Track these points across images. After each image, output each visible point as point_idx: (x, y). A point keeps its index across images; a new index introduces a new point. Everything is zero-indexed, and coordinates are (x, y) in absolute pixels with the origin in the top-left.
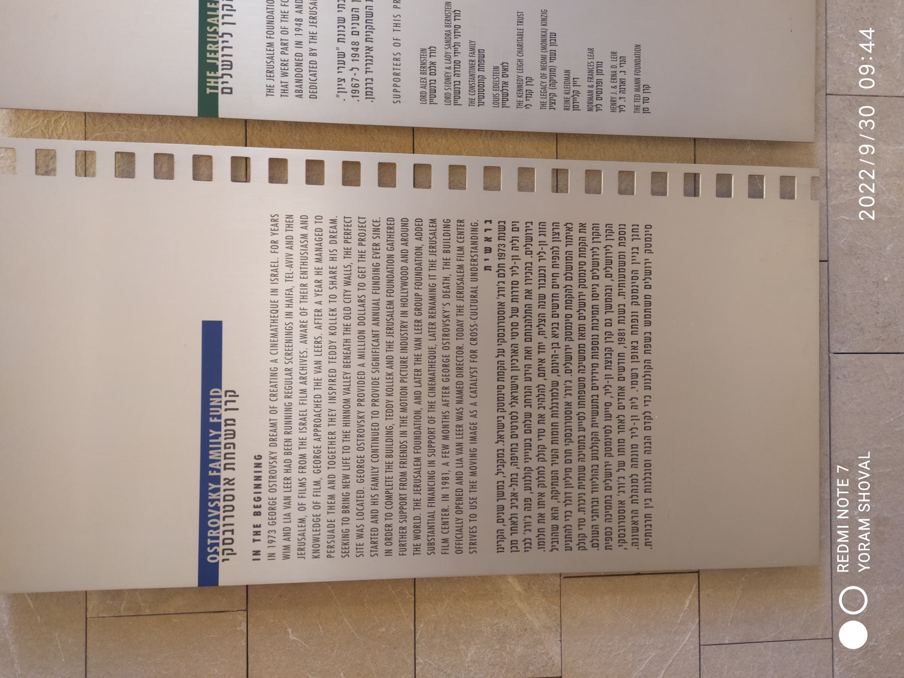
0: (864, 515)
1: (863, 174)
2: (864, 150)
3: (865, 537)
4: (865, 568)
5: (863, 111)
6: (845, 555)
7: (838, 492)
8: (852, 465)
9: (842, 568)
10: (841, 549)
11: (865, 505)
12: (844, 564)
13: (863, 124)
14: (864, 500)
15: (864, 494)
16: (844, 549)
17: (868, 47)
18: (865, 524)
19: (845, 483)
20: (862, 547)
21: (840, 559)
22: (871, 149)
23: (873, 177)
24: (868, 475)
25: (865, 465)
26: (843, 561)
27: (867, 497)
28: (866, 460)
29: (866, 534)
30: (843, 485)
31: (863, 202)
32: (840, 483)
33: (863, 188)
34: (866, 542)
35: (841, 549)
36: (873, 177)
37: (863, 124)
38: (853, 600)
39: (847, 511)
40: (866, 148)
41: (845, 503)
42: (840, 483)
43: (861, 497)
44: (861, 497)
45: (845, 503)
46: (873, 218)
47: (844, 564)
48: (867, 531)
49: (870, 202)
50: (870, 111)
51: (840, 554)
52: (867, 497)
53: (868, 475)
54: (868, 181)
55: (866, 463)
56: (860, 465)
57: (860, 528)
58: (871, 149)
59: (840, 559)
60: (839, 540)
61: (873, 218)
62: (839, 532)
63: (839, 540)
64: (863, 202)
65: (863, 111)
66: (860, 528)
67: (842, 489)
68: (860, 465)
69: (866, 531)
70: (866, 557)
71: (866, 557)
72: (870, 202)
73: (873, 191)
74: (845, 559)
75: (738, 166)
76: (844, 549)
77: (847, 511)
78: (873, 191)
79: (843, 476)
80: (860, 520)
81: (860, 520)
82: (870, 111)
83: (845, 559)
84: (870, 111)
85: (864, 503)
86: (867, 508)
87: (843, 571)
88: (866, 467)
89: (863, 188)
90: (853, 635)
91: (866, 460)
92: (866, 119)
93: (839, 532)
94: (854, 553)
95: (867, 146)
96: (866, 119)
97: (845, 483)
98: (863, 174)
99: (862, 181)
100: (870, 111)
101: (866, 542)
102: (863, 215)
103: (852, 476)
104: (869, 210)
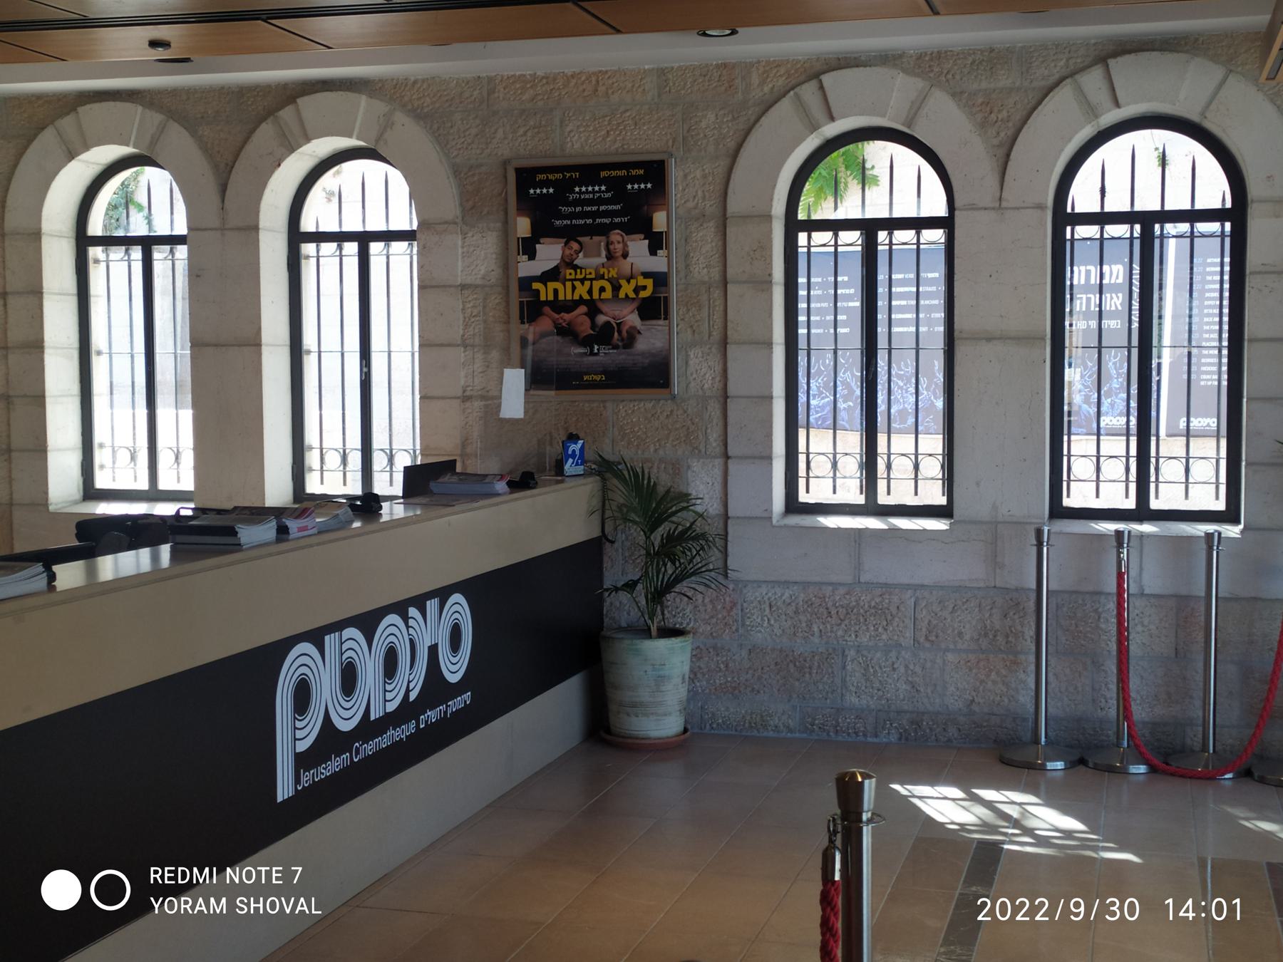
0: (231, 905)
1: (1042, 904)
2: (1077, 905)
3: (201, 906)
4: (157, 906)
5: (1132, 903)
6: (175, 878)
7: (263, 869)
8: (301, 891)
9: (155, 874)
10: (184, 873)
11: (246, 906)
12: (162, 877)
13: (1113, 904)
14: (252, 905)
15: (261, 905)
16: (184, 878)
17: (1187, 911)
18: (219, 906)
19: (277, 879)
20: (186, 902)
21: (169, 872)
22: (1077, 915)
23: (1038, 918)
24: (288, 911)
25: (302, 906)
26: (167, 875)
27: (257, 909)
28: (310, 909)
29: (204, 908)
30: (274, 875)
31: (1003, 904)
32: (277, 872)
33: (1023, 904)
34: (193, 908)
35: (184, 873)
36: (1038, 918)
37: (1113, 904)
38: (110, 890)
39: (237, 881)
40: (1078, 909)
41: (249, 878)
42: (277, 872)
43: (257, 902)
44: (257, 902)
45: (249, 878)
46: (980, 918)
47: (162, 877)
48: (208, 909)
49: (1003, 915)
50: (1132, 915)
51: (176, 872)
52: (257, 909)
53: (288, 911)
54: (1033, 911)
55: (305, 908)
56: (302, 900)
57: (212, 900)
58: (1077, 915)
59: (169, 872)
60: (195, 870)
61: (980, 918)
62: (207, 870)
63: (195, 870)
64: (1003, 904)
65: (1132, 903)
66: (212, 900)
67: (269, 874)
68: (302, 900)
69: (208, 909)
70: (171, 908)
71: (171, 908)
72: (1003, 915)
73: (1018, 918)
74: (169, 879)
75: (81, 702)
76: (184, 878)
77: (237, 881)
78: (1018, 918)
79: (287, 875)
80: (224, 900)
81: (224, 900)
82: (1132, 914)
83: (169, 879)
84: (1132, 915)
85: (248, 905)
86: (242, 909)
87: (152, 876)
88: (299, 908)
89: (1023, 904)
90: (60, 890)
91: (310, 909)
92: (1121, 908)
93: (207, 870)
94: (177, 891)
95: (1082, 909)
96: (1121, 908)
97: (277, 879)
98: (1042, 904)
99: (1032, 903)
100: (1132, 914)
101: (193, 908)
102: (984, 904)
103: (287, 890)
104: (991, 912)
